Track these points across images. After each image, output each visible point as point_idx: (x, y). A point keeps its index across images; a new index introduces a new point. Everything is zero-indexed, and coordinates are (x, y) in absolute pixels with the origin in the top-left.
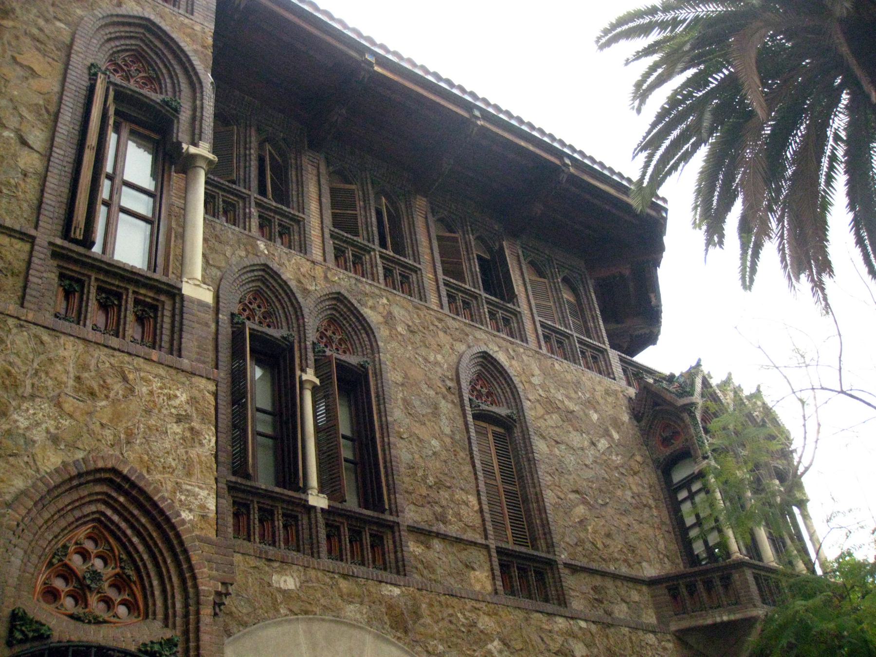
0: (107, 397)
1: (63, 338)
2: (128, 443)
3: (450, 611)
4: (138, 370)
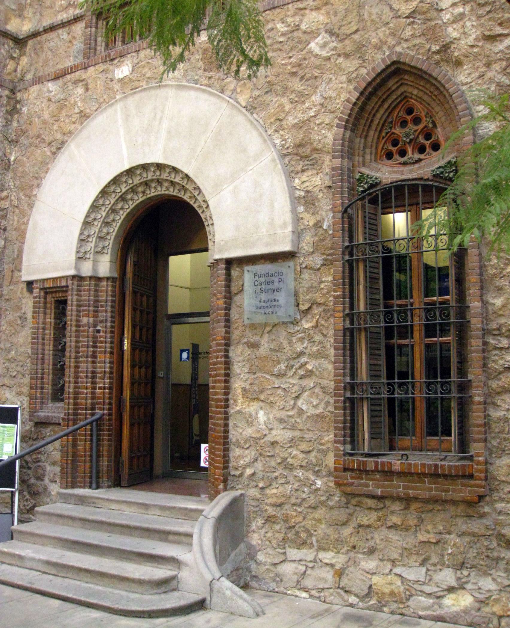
3: (270, 26)
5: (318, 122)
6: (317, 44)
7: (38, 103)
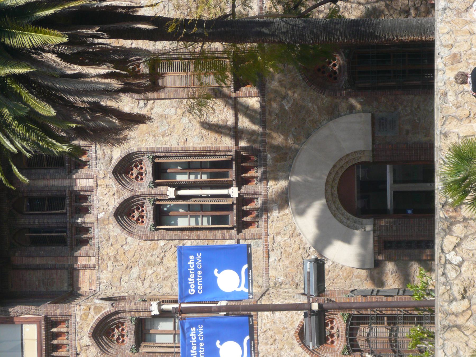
0: (274, 336)
1: (259, 350)
2: (287, 328)
4: (262, 327)
5: (320, 104)
6: (287, 105)
7: (279, 269)
